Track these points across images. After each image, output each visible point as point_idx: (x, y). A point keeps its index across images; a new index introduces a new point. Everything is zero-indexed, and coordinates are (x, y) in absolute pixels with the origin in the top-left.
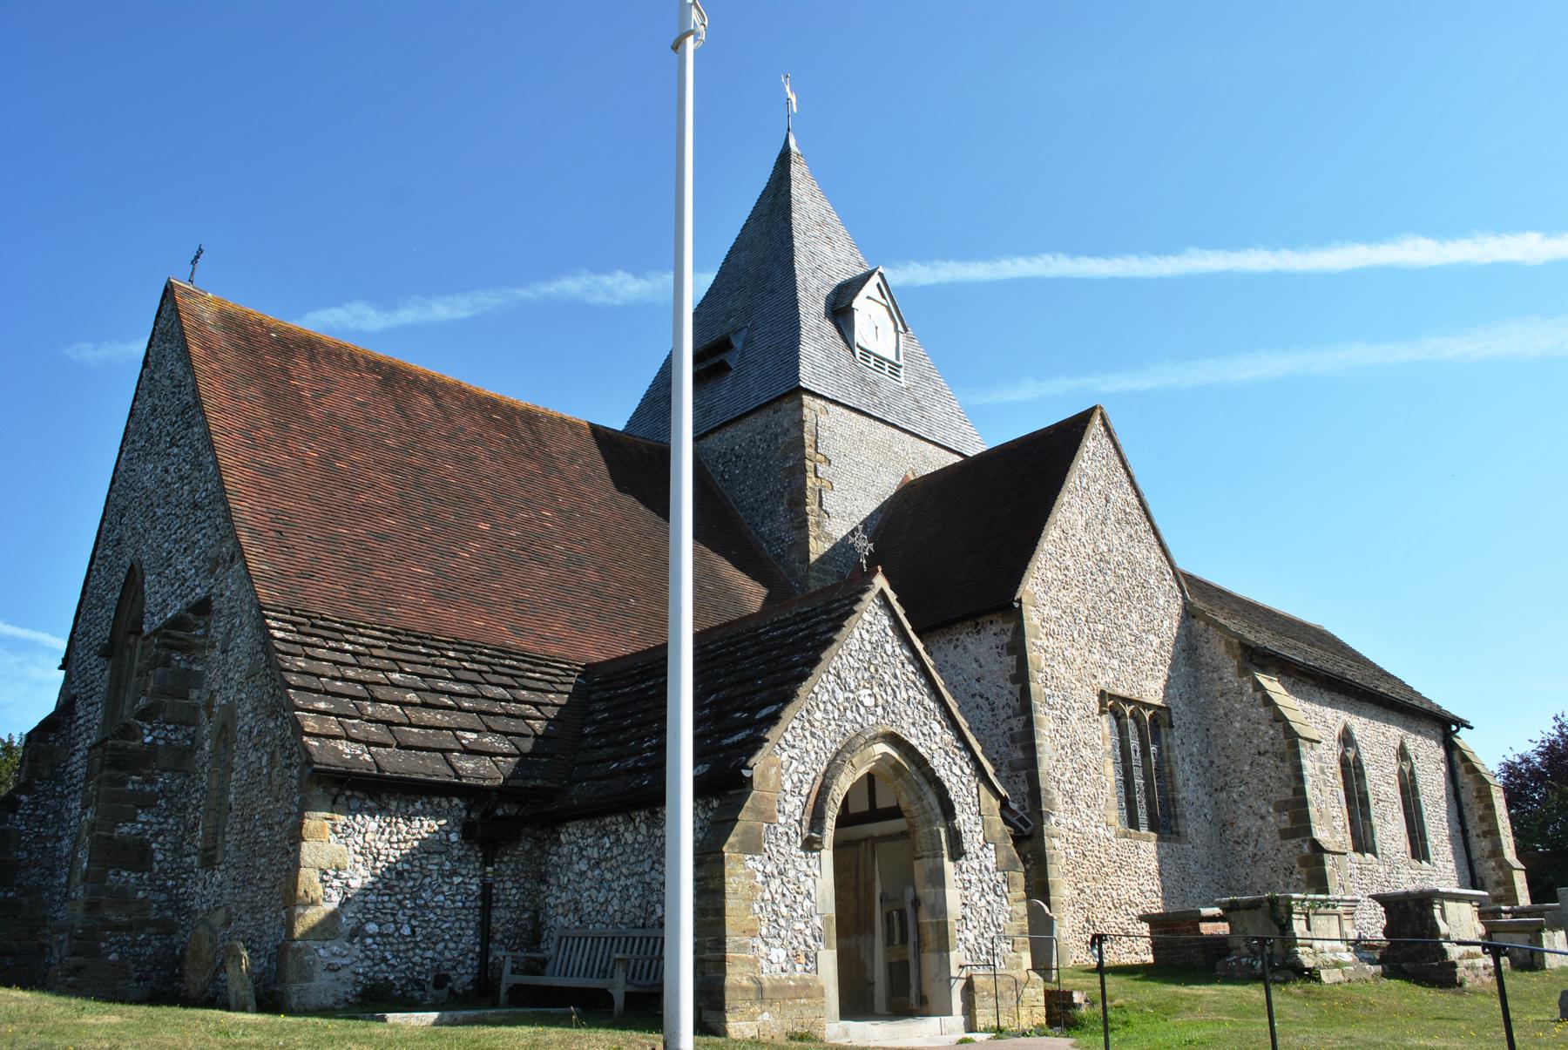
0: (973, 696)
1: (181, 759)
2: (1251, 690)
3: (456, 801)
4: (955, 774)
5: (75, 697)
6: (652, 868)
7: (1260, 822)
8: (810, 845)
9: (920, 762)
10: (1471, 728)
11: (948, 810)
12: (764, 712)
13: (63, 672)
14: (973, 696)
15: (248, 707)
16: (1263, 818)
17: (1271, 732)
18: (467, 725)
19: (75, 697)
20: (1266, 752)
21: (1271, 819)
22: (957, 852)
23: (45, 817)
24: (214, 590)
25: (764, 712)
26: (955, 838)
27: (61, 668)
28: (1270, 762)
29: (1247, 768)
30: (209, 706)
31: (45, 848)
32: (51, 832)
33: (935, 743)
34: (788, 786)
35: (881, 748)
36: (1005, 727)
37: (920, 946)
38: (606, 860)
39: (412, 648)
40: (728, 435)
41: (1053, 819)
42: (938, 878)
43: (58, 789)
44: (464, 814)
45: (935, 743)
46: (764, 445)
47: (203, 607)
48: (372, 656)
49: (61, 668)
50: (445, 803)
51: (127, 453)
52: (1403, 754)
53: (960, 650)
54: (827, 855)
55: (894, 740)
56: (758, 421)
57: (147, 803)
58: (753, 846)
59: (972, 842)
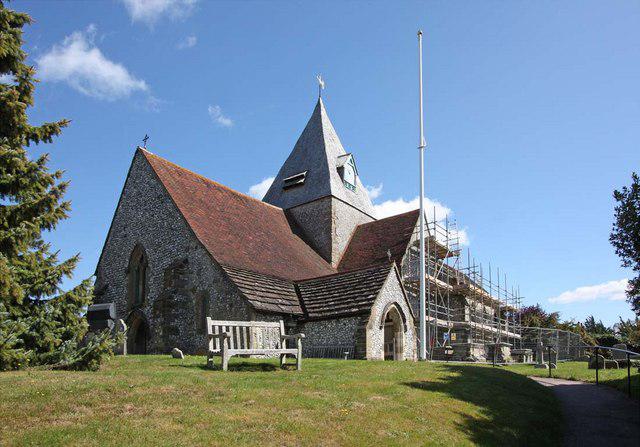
1: (184, 304)
4: (406, 311)
8: (381, 328)
9: (400, 309)
11: (404, 321)
22: (406, 330)
26: (406, 327)
30: (194, 290)
33: (403, 304)
35: (393, 306)
37: (397, 352)
42: (401, 336)
45: (403, 304)
47: (186, 261)
55: (396, 304)
56: (316, 204)
57: (176, 317)
58: (371, 328)
59: (408, 328)
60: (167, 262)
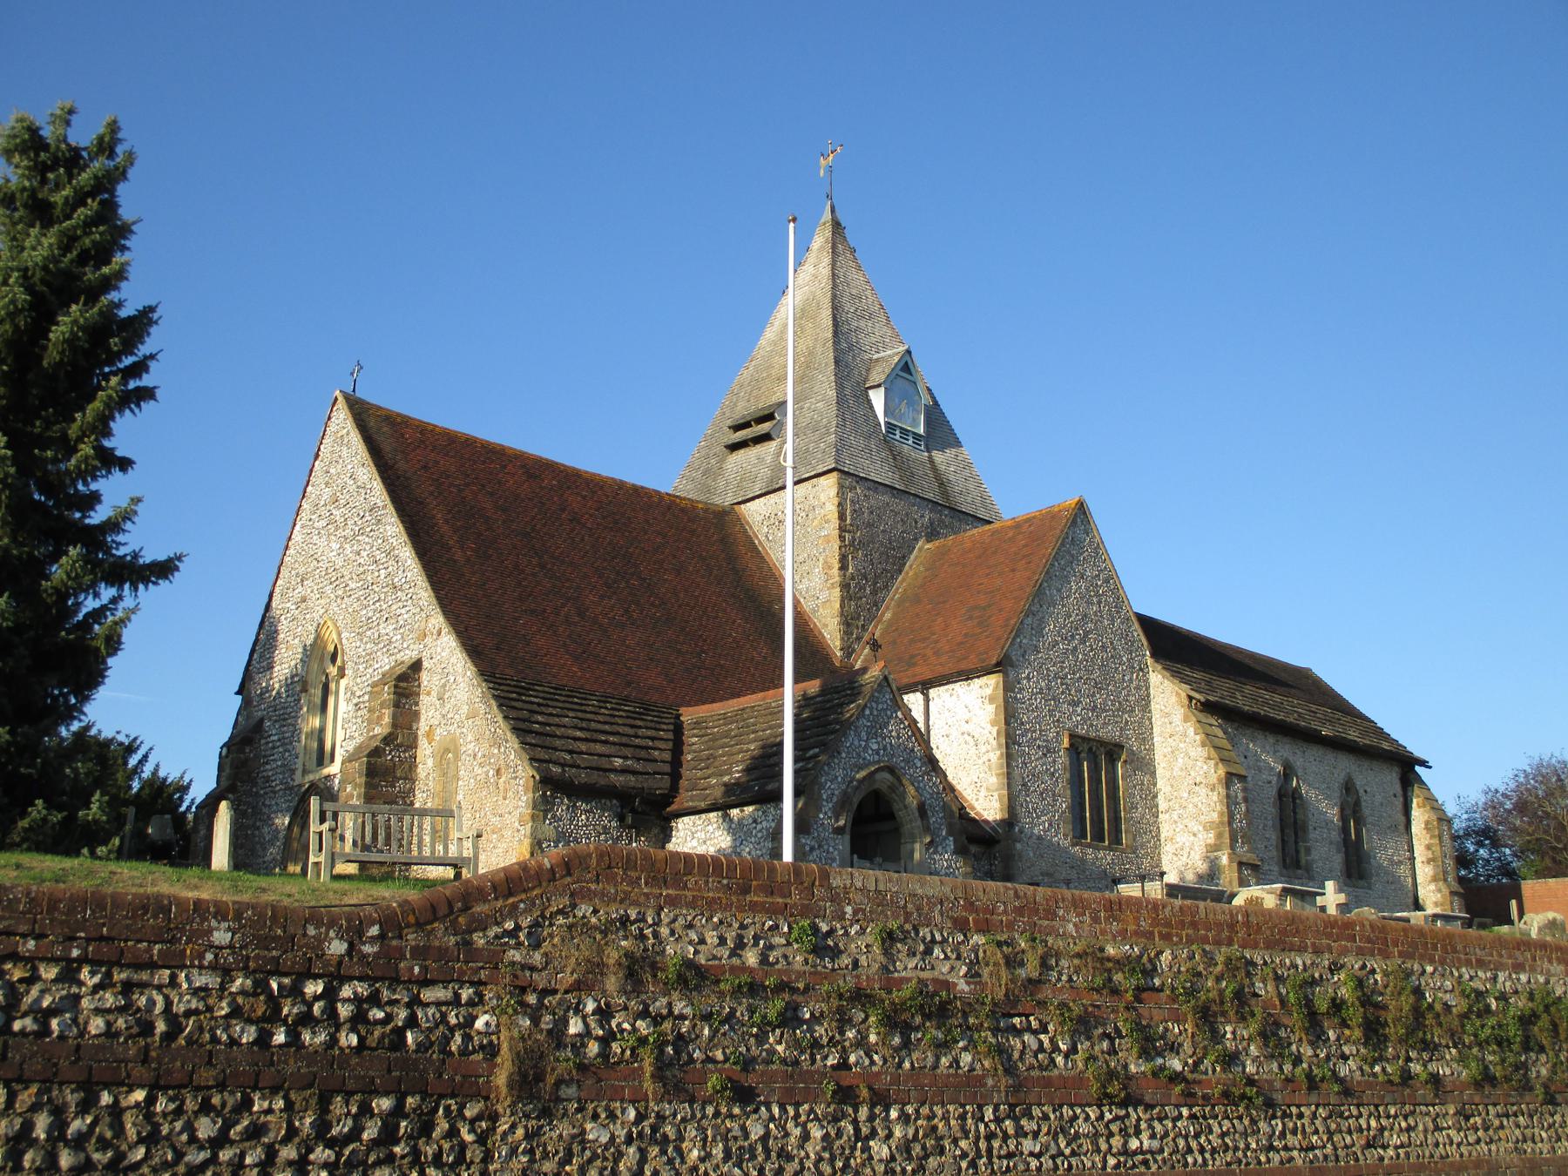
0: (963, 734)
2: (1192, 734)
3: (615, 801)
5: (262, 720)
6: (741, 844)
7: (1192, 838)
10: (1430, 767)
12: (811, 752)
13: (240, 697)
14: (963, 734)
15: (470, 738)
16: (1195, 835)
17: (1205, 767)
18: (619, 754)
19: (262, 720)
20: (1201, 783)
21: (1200, 836)
23: (246, 810)
24: (424, 654)
25: (811, 752)
27: (238, 693)
28: (1203, 791)
29: (1186, 795)
31: (247, 835)
32: (251, 822)
34: (825, 797)
36: (985, 758)
38: (710, 839)
39: (570, 700)
40: (772, 501)
41: (1017, 829)
43: (254, 790)
44: (619, 810)
46: (803, 514)
48: (549, 706)
49: (238, 693)
50: (608, 803)
51: (303, 527)
52: (1348, 787)
53: (954, 697)
54: (847, 837)
60: (385, 664)
